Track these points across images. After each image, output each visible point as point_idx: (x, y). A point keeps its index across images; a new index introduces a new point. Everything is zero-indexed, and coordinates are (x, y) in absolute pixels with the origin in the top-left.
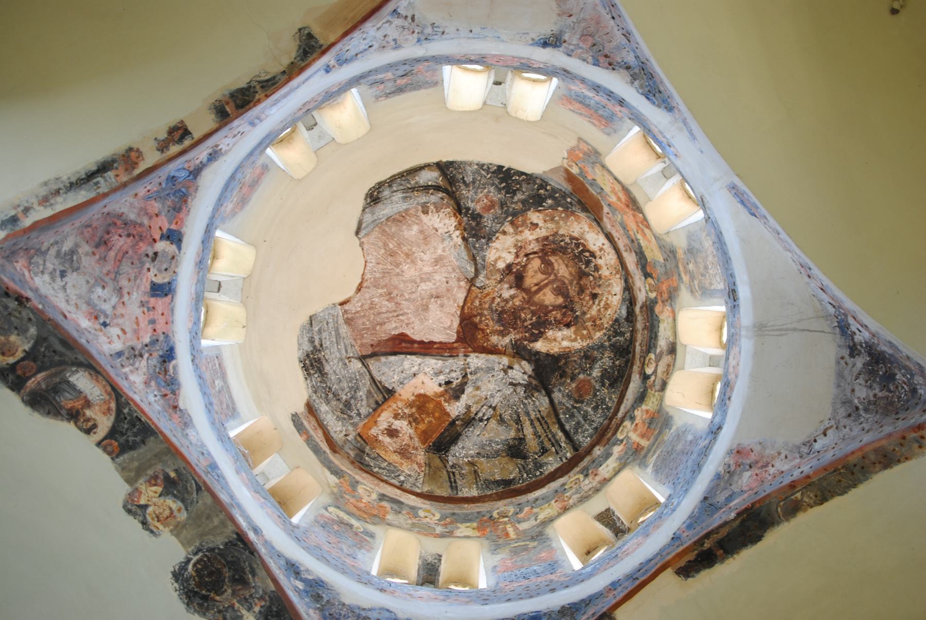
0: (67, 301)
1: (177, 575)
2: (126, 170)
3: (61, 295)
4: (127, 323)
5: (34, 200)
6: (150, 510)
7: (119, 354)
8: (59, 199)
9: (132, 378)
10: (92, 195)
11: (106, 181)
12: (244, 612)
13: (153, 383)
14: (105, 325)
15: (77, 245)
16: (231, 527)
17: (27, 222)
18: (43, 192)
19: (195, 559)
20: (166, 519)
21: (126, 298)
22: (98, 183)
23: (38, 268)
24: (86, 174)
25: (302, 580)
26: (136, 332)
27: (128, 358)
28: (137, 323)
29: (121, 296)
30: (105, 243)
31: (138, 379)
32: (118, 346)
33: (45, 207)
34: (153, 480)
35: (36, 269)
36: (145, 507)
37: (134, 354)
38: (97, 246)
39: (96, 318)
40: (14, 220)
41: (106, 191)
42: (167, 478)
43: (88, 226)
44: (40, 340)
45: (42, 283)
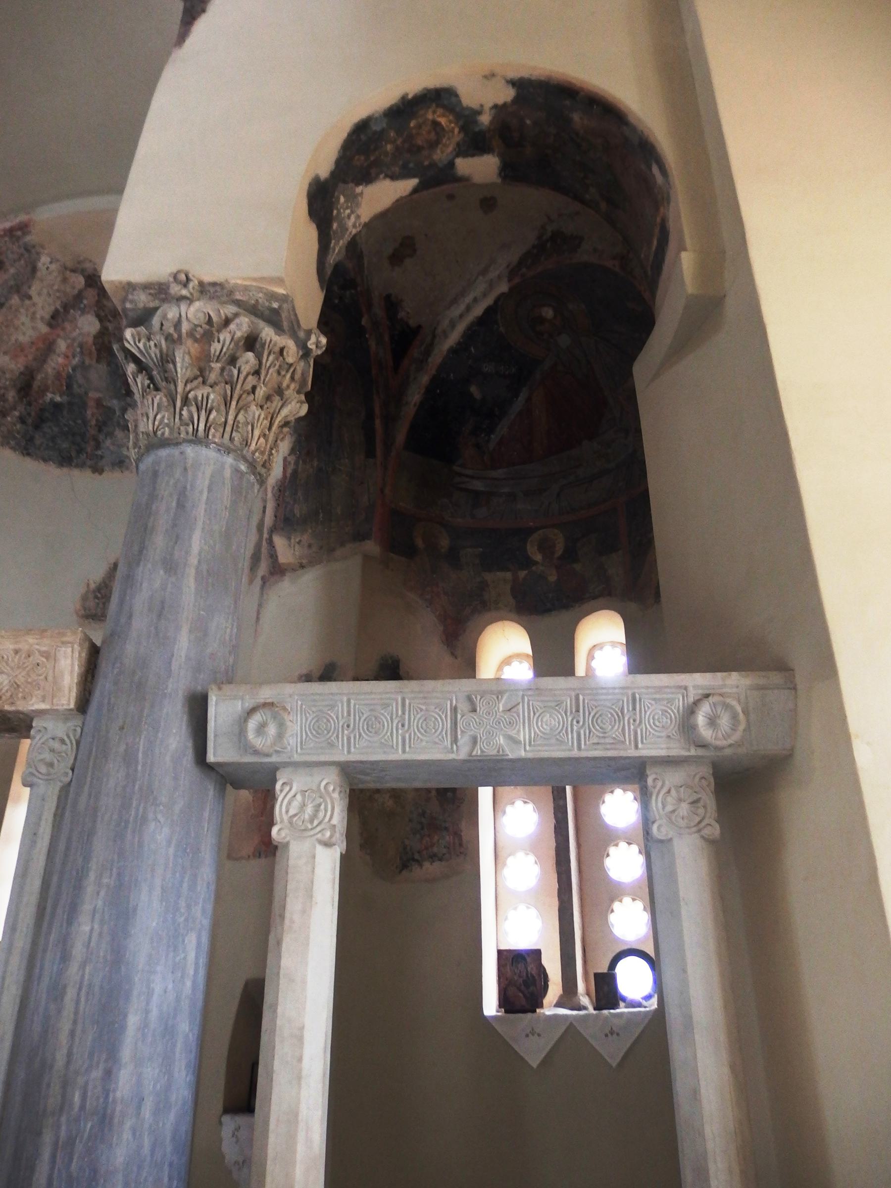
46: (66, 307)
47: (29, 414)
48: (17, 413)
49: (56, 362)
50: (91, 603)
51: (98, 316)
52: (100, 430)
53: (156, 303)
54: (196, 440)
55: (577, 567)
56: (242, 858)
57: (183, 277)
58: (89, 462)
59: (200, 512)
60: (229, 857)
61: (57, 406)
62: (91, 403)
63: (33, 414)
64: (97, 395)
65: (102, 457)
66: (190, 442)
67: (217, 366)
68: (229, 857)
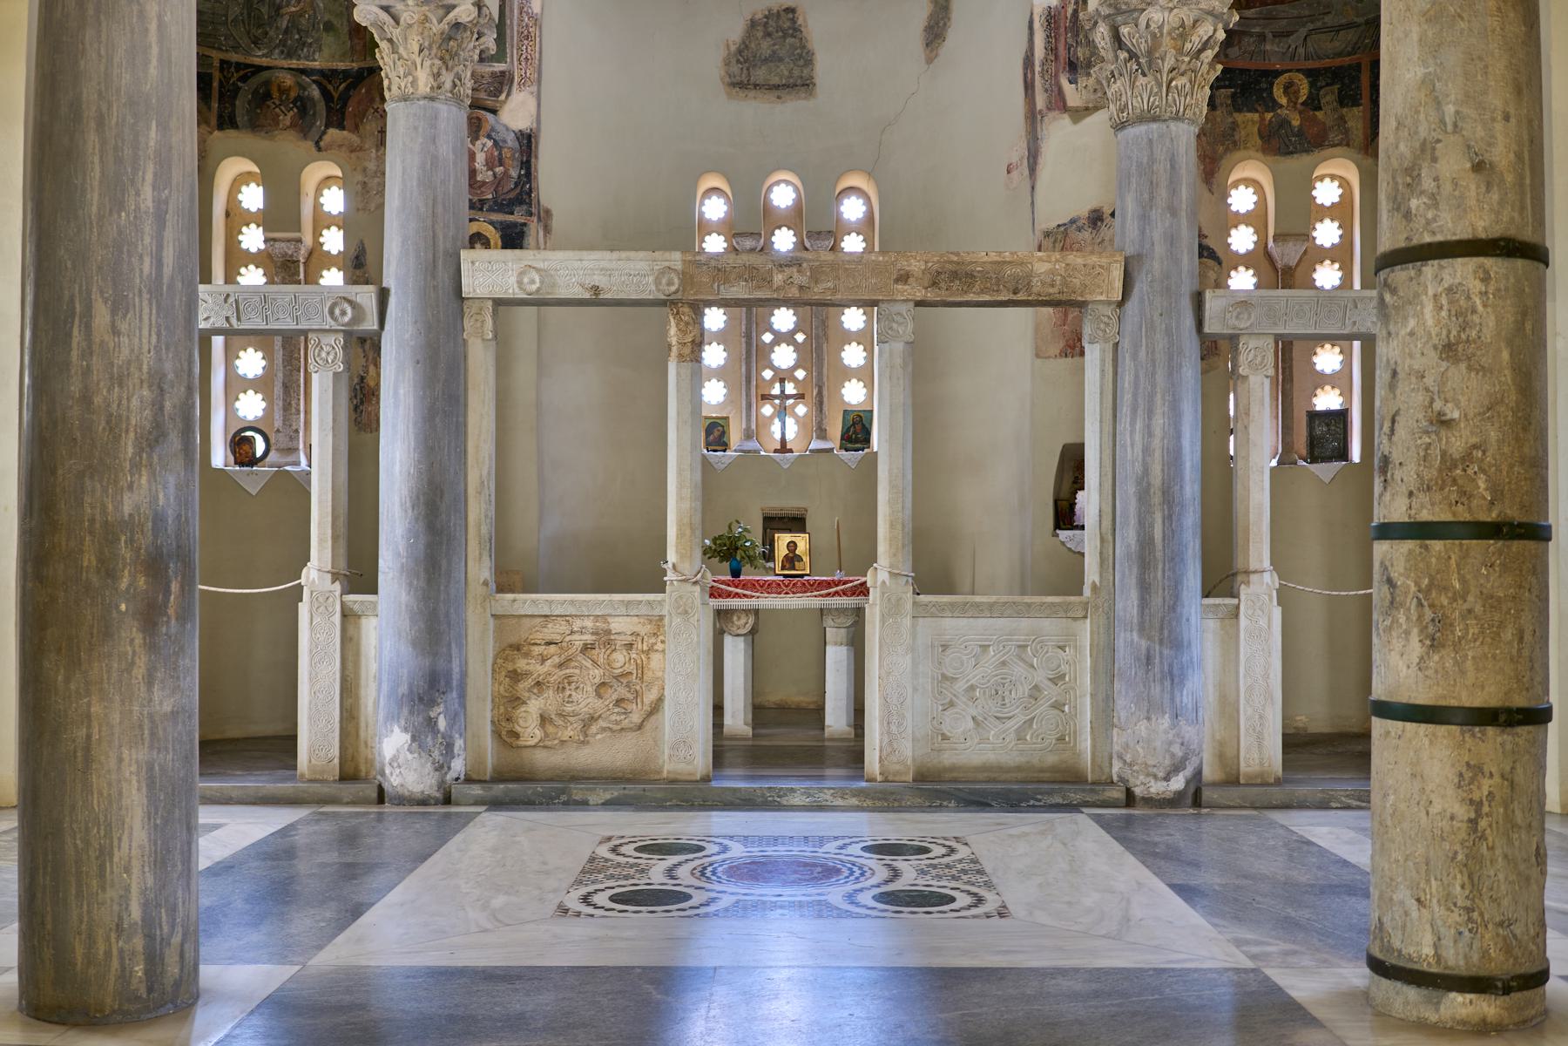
50: (735, 69)
54: (1177, 117)
55: (1319, 114)
59: (1183, 171)
60: (1037, 356)
67: (1187, 59)
68: (1037, 356)
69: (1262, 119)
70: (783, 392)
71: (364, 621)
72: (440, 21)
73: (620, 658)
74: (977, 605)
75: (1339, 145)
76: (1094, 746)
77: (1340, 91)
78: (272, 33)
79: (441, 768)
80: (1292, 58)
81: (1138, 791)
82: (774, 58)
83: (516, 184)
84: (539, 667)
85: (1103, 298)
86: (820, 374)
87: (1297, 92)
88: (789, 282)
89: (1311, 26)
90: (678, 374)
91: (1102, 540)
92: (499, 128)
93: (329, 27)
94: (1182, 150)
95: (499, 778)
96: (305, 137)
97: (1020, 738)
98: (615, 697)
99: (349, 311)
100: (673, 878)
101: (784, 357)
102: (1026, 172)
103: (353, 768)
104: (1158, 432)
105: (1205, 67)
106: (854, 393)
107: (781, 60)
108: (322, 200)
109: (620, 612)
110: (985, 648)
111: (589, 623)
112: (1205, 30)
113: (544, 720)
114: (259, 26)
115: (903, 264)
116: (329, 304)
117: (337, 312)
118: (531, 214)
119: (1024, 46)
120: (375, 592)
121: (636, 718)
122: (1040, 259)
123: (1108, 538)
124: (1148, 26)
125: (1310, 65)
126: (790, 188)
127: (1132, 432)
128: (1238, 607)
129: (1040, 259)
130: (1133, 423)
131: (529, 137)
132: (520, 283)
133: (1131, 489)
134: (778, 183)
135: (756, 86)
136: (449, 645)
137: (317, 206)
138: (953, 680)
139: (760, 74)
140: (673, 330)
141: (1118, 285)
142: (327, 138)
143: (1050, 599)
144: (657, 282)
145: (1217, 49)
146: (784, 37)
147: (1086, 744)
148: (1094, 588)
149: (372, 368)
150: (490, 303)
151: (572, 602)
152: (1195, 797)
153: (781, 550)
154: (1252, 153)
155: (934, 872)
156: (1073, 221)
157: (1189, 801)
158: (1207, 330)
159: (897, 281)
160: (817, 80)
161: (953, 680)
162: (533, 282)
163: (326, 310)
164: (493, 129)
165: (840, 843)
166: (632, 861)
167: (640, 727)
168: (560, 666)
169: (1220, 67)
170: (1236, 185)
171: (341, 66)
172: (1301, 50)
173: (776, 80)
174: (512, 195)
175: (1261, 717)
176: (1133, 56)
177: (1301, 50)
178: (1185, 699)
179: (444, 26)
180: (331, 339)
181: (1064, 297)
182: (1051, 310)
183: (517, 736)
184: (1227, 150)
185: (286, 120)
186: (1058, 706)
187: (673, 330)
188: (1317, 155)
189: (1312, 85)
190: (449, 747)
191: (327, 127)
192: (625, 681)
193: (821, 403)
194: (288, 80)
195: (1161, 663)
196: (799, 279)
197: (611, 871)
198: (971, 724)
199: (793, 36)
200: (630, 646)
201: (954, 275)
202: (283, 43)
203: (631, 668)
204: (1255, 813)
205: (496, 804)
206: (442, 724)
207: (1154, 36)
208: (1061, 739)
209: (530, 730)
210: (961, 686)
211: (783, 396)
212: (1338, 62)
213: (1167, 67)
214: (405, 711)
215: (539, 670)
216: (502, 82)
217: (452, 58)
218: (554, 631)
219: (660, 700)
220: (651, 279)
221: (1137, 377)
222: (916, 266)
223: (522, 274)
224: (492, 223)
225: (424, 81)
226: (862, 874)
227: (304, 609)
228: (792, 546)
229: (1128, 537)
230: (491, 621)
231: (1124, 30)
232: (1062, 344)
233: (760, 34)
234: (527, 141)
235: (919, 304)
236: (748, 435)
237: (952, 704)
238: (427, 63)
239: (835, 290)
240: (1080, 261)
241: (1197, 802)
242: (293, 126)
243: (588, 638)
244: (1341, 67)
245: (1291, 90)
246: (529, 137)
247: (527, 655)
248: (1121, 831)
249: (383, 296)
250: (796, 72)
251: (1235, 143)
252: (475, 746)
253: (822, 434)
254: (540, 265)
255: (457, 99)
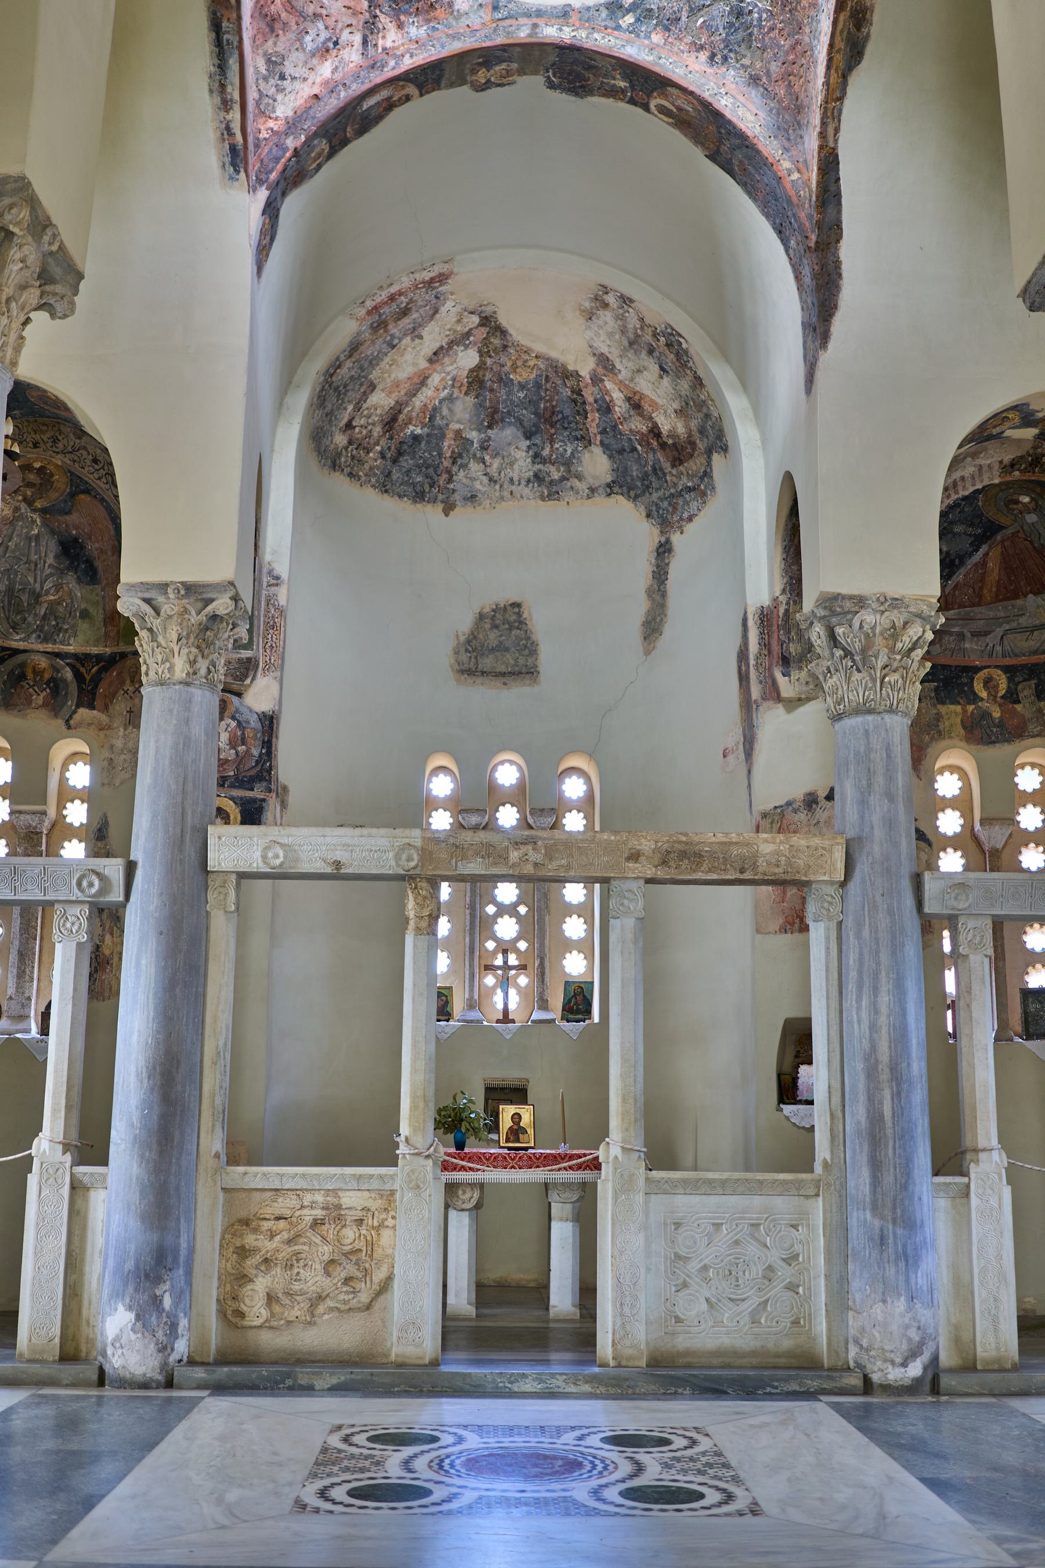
0: (305, 80)
1: (551, 86)
2: (227, 8)
3: (297, 85)
4: (344, 19)
5: (222, 114)
6: (493, 79)
7: (365, 42)
8: (229, 89)
9: (389, 44)
10: (236, 56)
11: (228, 32)
12: (613, 82)
13: (402, 18)
14: (336, 43)
15: (265, 54)
16: (549, 49)
17: (239, 138)
18: (217, 100)
19: (551, 74)
20: (509, 73)
21: (324, 12)
22: (228, 40)
23: (268, 104)
24: (216, 46)
25: (628, 11)
26: (356, 13)
27: (372, 33)
28: (349, 8)
29: (321, 15)
30: (273, 20)
31: (391, 37)
32: (357, 38)
33: (231, 108)
34: (474, 72)
35: (270, 108)
36: (488, 81)
37: (371, 27)
38: (272, 30)
39: (327, 51)
40: (233, 149)
41: (237, 38)
42: (480, 64)
43: (254, 42)
44: (324, 136)
45: (284, 109)
46: (451, 344)
47: (389, 448)
48: (378, 448)
49: (426, 396)
50: (464, 657)
51: (479, 351)
52: (453, 463)
53: (856, 609)
54: (891, 710)
55: (1019, 707)
56: (769, 933)
57: (882, 599)
58: (440, 497)
59: (899, 760)
60: (758, 931)
61: (416, 438)
62: (450, 435)
63: (393, 447)
64: (457, 426)
65: (454, 491)
66: (888, 711)
67: (898, 657)
68: (758, 931)
69: (965, 711)
70: (506, 962)
71: (92, 1193)
72: (199, 613)
73: (349, 1234)
74: (709, 1182)
75: (1037, 736)
76: (829, 1330)
77: (1037, 686)
78: (30, 619)
79: (164, 1349)
80: (991, 655)
81: (876, 1377)
82: (501, 648)
83: (257, 763)
84: (267, 1243)
85: (826, 878)
86: (542, 945)
87: (996, 687)
88: (524, 859)
89: (1007, 627)
90: (415, 946)
91: (832, 1116)
92: (242, 709)
93: (85, 615)
94: (897, 740)
95: (223, 1359)
96: (56, 716)
97: (755, 1322)
98: (343, 1275)
99: (96, 883)
100: (410, 1471)
101: (507, 928)
102: (742, 756)
103: (73, 1349)
104: (884, 1009)
105: (916, 665)
106: (575, 965)
107: (507, 649)
108: (67, 775)
109: (351, 1186)
110: (718, 1226)
111: (319, 1198)
112: (915, 631)
113: (271, 1299)
114: (19, 613)
115: (634, 843)
116: (77, 876)
117: (85, 884)
118: (270, 791)
119: (737, 641)
120: (105, 1162)
121: (364, 1297)
122: (766, 841)
123: (838, 1115)
124: (861, 627)
125: (1008, 661)
126: (514, 768)
127: (859, 1009)
128: (968, 1186)
129: (766, 841)
130: (859, 1000)
131: (271, 718)
132: (264, 857)
133: (860, 1066)
134: (502, 763)
135: (483, 673)
136: (178, 1219)
137: (63, 780)
138: (686, 1259)
139: (487, 662)
140: (411, 904)
141: (841, 865)
142: (77, 717)
143: (782, 1176)
144: (397, 858)
145: (926, 648)
146: (510, 629)
147: (821, 1327)
148: (826, 1165)
149: (108, 937)
150: (233, 877)
151: (304, 1176)
152: (932, 1383)
153: (506, 1122)
154: (956, 742)
155: (678, 1466)
156: (789, 804)
157: (927, 1388)
158: (927, 910)
159: (629, 859)
160: (541, 669)
161: (686, 1259)
162: (277, 856)
163: (74, 882)
164: (237, 711)
165: (578, 1433)
166: (365, 1452)
167: (368, 1307)
168: (289, 1242)
169: (929, 665)
170: (941, 772)
171: (95, 650)
172: (999, 648)
173: (502, 668)
174: (253, 772)
175: (996, 1300)
176: (847, 654)
177: (999, 648)
178: (920, 1281)
179: (202, 617)
180: (76, 910)
181: (788, 877)
182: (770, 888)
183: (242, 1315)
184: (932, 739)
185: (39, 699)
186: (792, 1287)
187: (411, 904)
188: (1017, 745)
189: (1010, 680)
190: (173, 1326)
191: (78, 706)
192: (354, 1259)
193: (542, 974)
194: (43, 663)
195: (895, 1243)
196: (534, 856)
197: (346, 1463)
198: (705, 1306)
199: (518, 628)
200: (360, 1222)
201: (683, 855)
202: (40, 628)
203: (361, 1244)
204: (993, 1400)
205: (219, 1389)
206: (167, 1302)
207: (867, 635)
208: (796, 1322)
209: (256, 1310)
210: (694, 1266)
211: (506, 967)
212: (1034, 659)
213: (880, 664)
214: (131, 1289)
215: (268, 1246)
216: (245, 669)
217: (208, 646)
218: (284, 1205)
219: (390, 1278)
220: (391, 855)
221: (861, 954)
222: (646, 845)
223: (267, 848)
224: (232, 799)
225: (180, 667)
226: (605, 1468)
227: (33, 1181)
228: (517, 1118)
229: (858, 1114)
230: (221, 1196)
231: (840, 631)
232: (781, 921)
233: (488, 626)
234: (269, 722)
235: (649, 881)
236: (471, 1005)
237: (685, 1285)
238: (185, 651)
239: (568, 867)
240: (803, 843)
241: (935, 1389)
242: (45, 705)
243: (319, 1213)
244: (1037, 664)
245: (991, 684)
246: (271, 718)
247: (256, 1230)
248: (861, 1419)
249: (131, 868)
250: (521, 661)
251: (939, 733)
252: (199, 1327)
253: (544, 1005)
254: (284, 840)
255: (211, 684)
